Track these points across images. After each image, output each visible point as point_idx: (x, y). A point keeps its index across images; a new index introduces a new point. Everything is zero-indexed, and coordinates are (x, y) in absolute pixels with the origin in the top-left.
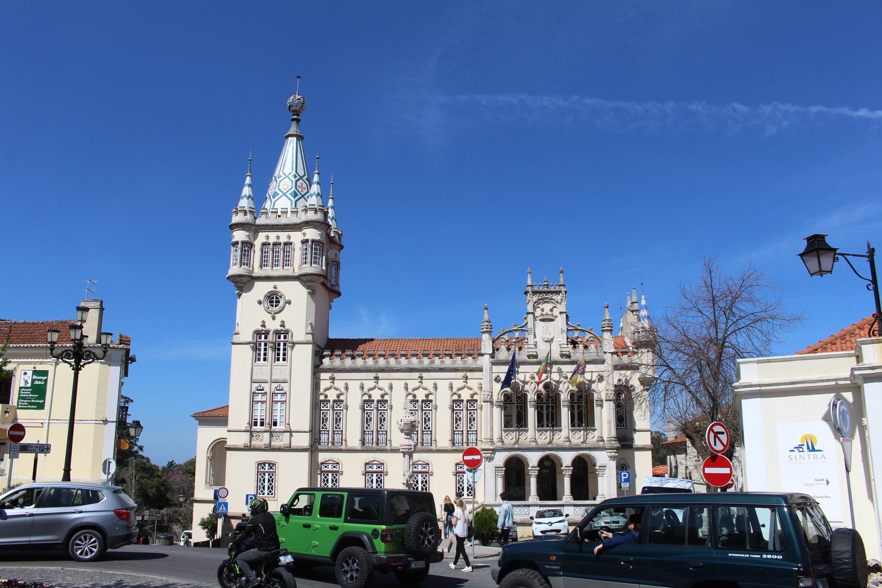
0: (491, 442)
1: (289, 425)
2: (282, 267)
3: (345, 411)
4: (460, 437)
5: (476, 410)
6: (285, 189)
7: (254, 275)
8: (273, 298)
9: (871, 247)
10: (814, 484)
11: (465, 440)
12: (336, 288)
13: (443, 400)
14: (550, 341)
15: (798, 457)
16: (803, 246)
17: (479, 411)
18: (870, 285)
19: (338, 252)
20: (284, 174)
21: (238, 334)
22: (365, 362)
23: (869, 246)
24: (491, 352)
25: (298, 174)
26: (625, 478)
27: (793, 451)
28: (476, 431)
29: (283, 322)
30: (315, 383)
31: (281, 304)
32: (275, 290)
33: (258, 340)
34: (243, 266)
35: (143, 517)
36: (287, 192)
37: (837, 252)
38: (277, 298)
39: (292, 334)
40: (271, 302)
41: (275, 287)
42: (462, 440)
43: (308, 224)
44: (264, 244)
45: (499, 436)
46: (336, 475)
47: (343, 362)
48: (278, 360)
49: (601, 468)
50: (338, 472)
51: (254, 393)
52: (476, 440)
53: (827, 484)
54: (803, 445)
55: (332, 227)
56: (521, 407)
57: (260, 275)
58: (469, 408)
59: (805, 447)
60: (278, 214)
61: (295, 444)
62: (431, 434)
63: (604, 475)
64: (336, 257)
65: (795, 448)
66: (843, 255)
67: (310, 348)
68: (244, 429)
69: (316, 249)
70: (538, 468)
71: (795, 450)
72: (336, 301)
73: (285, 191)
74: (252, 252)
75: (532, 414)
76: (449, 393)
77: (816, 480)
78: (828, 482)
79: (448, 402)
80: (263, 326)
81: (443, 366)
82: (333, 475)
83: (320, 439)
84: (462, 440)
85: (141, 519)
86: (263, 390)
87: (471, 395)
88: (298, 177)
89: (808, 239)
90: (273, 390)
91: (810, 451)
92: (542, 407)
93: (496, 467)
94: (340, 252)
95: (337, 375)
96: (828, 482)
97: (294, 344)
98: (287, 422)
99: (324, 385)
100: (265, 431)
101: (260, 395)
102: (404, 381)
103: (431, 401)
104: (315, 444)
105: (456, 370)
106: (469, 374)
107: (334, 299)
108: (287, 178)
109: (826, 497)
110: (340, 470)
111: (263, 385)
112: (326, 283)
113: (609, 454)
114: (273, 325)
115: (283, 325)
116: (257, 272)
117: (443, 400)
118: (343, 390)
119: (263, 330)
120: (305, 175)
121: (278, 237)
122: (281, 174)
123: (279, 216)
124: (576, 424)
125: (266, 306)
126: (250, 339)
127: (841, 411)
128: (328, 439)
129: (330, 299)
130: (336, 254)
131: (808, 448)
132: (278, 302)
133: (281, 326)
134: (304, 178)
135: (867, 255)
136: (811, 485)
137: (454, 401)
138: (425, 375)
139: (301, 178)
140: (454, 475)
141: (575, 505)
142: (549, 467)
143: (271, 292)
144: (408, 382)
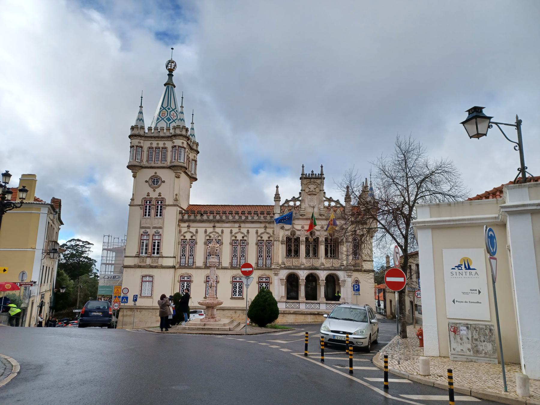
0: (278, 264)
1: (162, 253)
2: (160, 162)
3: (195, 245)
5: (271, 246)
6: (163, 116)
7: (143, 166)
8: (155, 180)
9: (519, 119)
10: (469, 293)
12: (194, 176)
13: (252, 240)
14: (314, 207)
15: (458, 274)
16: (466, 116)
17: (273, 247)
18: (517, 146)
19: (196, 155)
21: (133, 200)
23: (517, 117)
24: (279, 212)
25: (171, 107)
26: (357, 288)
27: (454, 269)
28: (271, 258)
29: (160, 193)
30: (178, 229)
31: (159, 183)
32: (156, 175)
34: (136, 160)
36: (164, 118)
37: (492, 120)
38: (157, 179)
39: (165, 201)
40: (153, 182)
41: (156, 173)
42: (263, 263)
43: (175, 136)
44: (150, 148)
45: (283, 261)
46: (189, 283)
48: (157, 215)
49: (342, 282)
50: (190, 281)
52: (271, 263)
53: (479, 294)
54: (462, 265)
55: (192, 141)
56: (297, 245)
57: (147, 166)
58: (267, 245)
59: (463, 266)
60: (158, 130)
61: (164, 264)
62: (245, 259)
63: (345, 286)
65: (456, 267)
66: (496, 124)
67: (176, 210)
68: (135, 255)
70: (306, 281)
71: (455, 268)
72: (194, 183)
73: (163, 117)
74: (143, 152)
75: (303, 248)
76: (255, 235)
77: (471, 290)
78: (479, 292)
79: (255, 241)
80: (148, 195)
81: (253, 220)
82: (187, 283)
83: (180, 262)
84: (263, 263)
86: (147, 233)
87: (268, 237)
88: (171, 109)
89: (469, 111)
90: (153, 233)
91: (467, 269)
92: (309, 246)
93: (280, 279)
94: (197, 155)
95: (192, 224)
96: (479, 292)
97: (166, 206)
99: (184, 230)
100: (147, 257)
101: (145, 236)
102: (230, 229)
103: (246, 240)
105: (261, 222)
106: (267, 225)
107: (193, 182)
108: (164, 110)
109: (478, 302)
110: (192, 280)
111: (148, 230)
112: (188, 172)
113: (347, 274)
114: (154, 195)
115: (160, 195)
116: (145, 163)
117: (252, 240)
118: (195, 233)
119: (148, 198)
120: (176, 108)
121: (158, 144)
122: (162, 107)
123: (159, 132)
124: (329, 256)
125: (150, 184)
126: (140, 203)
127: (490, 235)
128: (185, 262)
129: (191, 182)
130: (195, 156)
131: (465, 267)
133: (159, 196)
134: (175, 110)
135: (516, 124)
136: (467, 293)
137: (259, 240)
138: (242, 225)
139: (173, 110)
140: (257, 284)
141: (326, 304)
142: (312, 279)
144: (233, 229)
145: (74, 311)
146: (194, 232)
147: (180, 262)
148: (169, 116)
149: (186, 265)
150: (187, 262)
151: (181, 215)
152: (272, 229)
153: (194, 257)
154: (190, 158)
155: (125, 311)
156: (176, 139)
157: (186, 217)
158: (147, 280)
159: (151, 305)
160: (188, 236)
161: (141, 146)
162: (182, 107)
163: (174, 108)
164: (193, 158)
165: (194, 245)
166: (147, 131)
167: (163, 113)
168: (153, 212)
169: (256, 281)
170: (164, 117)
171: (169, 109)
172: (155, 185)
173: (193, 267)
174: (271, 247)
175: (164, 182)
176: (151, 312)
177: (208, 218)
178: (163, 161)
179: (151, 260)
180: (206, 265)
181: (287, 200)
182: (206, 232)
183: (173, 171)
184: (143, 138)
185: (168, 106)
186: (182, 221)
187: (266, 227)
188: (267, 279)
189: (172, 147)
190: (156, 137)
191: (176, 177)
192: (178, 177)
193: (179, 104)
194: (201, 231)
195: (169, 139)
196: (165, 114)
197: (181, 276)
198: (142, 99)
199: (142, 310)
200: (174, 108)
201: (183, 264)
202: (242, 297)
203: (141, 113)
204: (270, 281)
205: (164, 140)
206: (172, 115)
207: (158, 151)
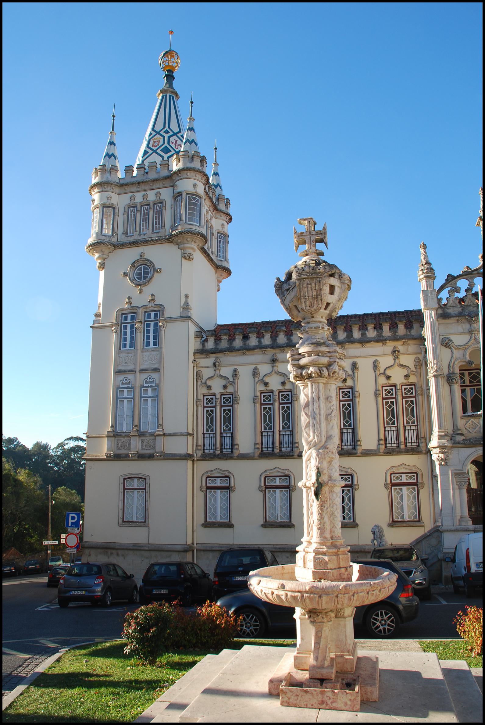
1: (162, 425)
2: (151, 231)
3: (236, 406)
4: (394, 435)
5: (415, 397)
6: (155, 146)
8: (141, 269)
11: (402, 439)
12: (225, 264)
17: (420, 398)
19: (226, 224)
20: (155, 131)
22: (260, 342)
29: (152, 295)
33: (123, 321)
35: (60, 541)
38: (145, 268)
47: (231, 344)
48: (148, 344)
50: (228, 488)
51: (118, 388)
52: (418, 438)
60: (146, 171)
64: (222, 228)
69: (190, 204)
73: (155, 149)
84: (398, 439)
85: (57, 543)
88: (171, 133)
95: (224, 359)
98: (160, 423)
99: (207, 373)
101: (126, 390)
103: (351, 388)
104: (197, 451)
108: (158, 136)
110: (232, 485)
111: (130, 377)
118: (231, 379)
120: (180, 132)
122: (153, 132)
123: (147, 173)
130: (223, 225)
132: (147, 273)
134: (179, 135)
139: (175, 134)
143: (138, 260)
145: (44, 544)
146: (229, 375)
147: (204, 445)
148: (166, 144)
149: (218, 452)
150: (218, 445)
151: (199, 340)
152: (414, 357)
153: (232, 433)
154: (213, 227)
155: (93, 552)
156: (181, 179)
157: (210, 344)
158: (135, 487)
159: (145, 541)
160: (217, 387)
161: (113, 204)
162: (192, 119)
163: (176, 130)
164: (220, 228)
165: (232, 406)
166: (121, 174)
167: (155, 142)
168: (139, 337)
169: (383, 482)
170: (157, 148)
171: (167, 132)
172: (142, 281)
173: (232, 455)
174: (414, 399)
175: (158, 272)
176: (147, 558)
177: (260, 342)
178: (156, 230)
179: (140, 441)
180: (262, 451)
181: (449, 275)
182: (255, 373)
183: (177, 246)
184: (117, 190)
185: (164, 127)
186: (202, 352)
187: (398, 351)
188: (410, 477)
189: (174, 196)
190: (143, 182)
191: (185, 258)
192: (188, 257)
193: (186, 125)
194: (245, 372)
195: (168, 183)
196: (159, 142)
197: (207, 478)
198: (114, 120)
199: (127, 552)
200: (176, 130)
201: (211, 451)
202: (352, 520)
203: (111, 143)
204: (420, 481)
205: (158, 186)
206: (172, 143)
207: (145, 212)
